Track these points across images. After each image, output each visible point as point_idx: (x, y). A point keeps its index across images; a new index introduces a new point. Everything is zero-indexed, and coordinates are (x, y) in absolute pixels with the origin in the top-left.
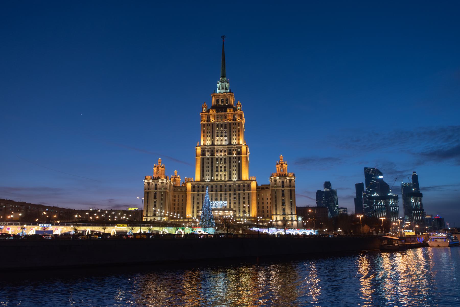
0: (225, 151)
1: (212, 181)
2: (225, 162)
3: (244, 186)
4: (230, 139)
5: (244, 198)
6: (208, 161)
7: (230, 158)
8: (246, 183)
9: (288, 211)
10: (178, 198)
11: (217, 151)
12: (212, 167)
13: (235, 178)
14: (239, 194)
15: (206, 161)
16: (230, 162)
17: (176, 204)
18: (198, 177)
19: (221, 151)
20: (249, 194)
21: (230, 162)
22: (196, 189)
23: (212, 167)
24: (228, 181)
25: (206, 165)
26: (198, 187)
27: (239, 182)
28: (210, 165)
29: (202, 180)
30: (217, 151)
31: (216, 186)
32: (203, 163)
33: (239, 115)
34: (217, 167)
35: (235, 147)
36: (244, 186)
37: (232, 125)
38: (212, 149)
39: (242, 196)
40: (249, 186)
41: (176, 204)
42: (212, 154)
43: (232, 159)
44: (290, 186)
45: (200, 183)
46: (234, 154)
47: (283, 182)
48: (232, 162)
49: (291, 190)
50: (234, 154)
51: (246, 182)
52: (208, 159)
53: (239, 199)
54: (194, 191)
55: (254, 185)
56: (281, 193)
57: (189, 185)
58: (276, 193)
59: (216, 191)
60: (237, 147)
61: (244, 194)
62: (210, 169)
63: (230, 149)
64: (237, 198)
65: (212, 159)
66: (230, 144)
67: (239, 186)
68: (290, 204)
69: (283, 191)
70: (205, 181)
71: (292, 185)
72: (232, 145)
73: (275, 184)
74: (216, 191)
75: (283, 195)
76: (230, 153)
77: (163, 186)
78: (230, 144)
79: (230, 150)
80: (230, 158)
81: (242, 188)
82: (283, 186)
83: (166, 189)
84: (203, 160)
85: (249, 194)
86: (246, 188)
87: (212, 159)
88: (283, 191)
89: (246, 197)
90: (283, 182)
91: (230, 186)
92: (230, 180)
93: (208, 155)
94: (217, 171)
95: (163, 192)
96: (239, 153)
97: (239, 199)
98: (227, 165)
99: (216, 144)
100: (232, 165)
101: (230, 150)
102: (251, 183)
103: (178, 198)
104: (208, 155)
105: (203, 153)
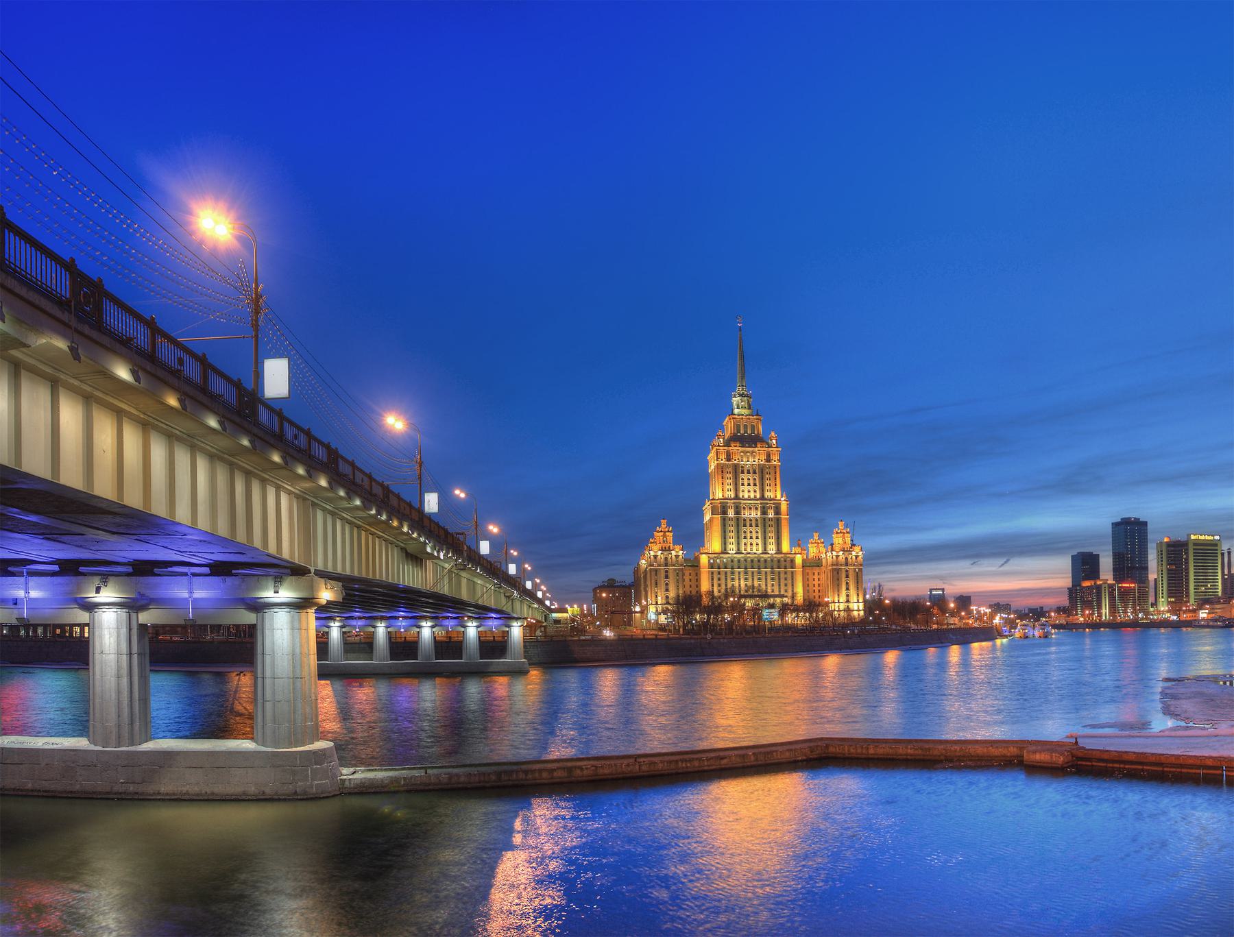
1: (739, 552)
4: (762, 490)
13: (772, 548)
18: (716, 546)
29: (724, 551)
40: (792, 561)
46: (771, 514)
50: (771, 514)
55: (799, 560)
56: (844, 575)
57: (704, 559)
66: (762, 498)
67: (779, 561)
76: (764, 513)
78: (762, 498)
81: (783, 564)
84: (724, 522)
89: (789, 576)
91: (766, 561)
92: (765, 552)
93: (731, 513)
96: (778, 512)
104: (731, 513)
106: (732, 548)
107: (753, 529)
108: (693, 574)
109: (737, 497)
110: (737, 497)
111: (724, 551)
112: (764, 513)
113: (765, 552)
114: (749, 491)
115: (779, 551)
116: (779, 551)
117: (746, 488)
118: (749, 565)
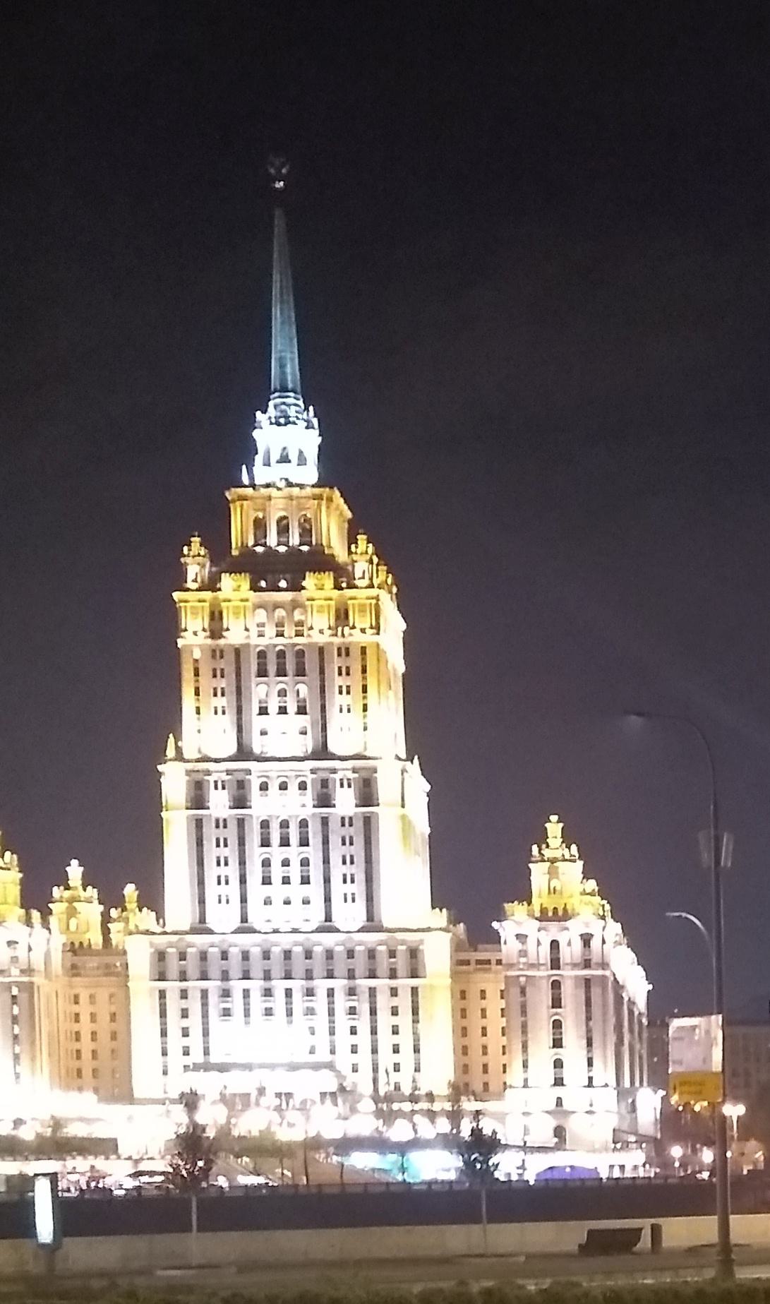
0: (303, 786)
2: (304, 842)
3: (392, 954)
5: (395, 1012)
6: (222, 833)
7: (325, 821)
8: (403, 942)
9: (575, 1070)
10: (94, 1027)
11: (264, 787)
12: (242, 863)
13: (350, 915)
14: (372, 992)
15: (210, 833)
16: (326, 842)
17: (86, 1055)
19: (283, 787)
20: (414, 991)
21: (326, 842)
22: (173, 966)
23: (242, 863)
24: (320, 930)
25: (211, 853)
26: (183, 957)
27: (372, 938)
28: (231, 852)
29: (201, 927)
30: (264, 787)
31: (266, 955)
32: (200, 843)
33: (362, 609)
34: (266, 863)
35: (345, 770)
36: (392, 954)
37: (335, 662)
38: (240, 776)
39: (383, 1002)
40: (414, 953)
41: (86, 1055)
42: (240, 802)
43: (334, 825)
44: (587, 964)
45: (189, 938)
46: (345, 802)
47: (555, 945)
48: (335, 840)
49: (588, 982)
50: (345, 802)
51: (399, 936)
52: (221, 824)
53: (373, 1012)
54: (162, 977)
56: (546, 996)
58: (523, 992)
59: (267, 976)
60: (354, 771)
61: (394, 992)
62: (232, 871)
63: (324, 775)
64: (364, 1008)
65: (241, 822)
66: (322, 752)
68: (585, 1041)
69: (556, 985)
70: (210, 932)
71: (595, 958)
72: (333, 757)
73: (523, 953)
74: (267, 976)
75: (557, 1003)
76: (324, 800)
77: (14, 959)
78: (322, 752)
79: (325, 783)
80: (325, 821)
81: (383, 963)
82: (555, 963)
83: (28, 971)
85: (414, 991)
86: (401, 963)
87: (241, 822)
88: (556, 985)
89: (404, 1002)
90: (555, 945)
91: (329, 955)
92: (328, 926)
93: (219, 803)
94: (267, 881)
95: (18, 984)
96: (367, 796)
97: (373, 1012)
98: (313, 852)
99: (257, 750)
100: (335, 859)
101: (325, 783)
102: (421, 942)
103: (94, 1027)
104: (219, 803)
105: (198, 800)
106: (223, 917)
107: (294, 852)
108: (102, 995)
109: (244, 753)
110: (244, 753)
111: (201, 927)
112: (324, 800)
113: (328, 926)
114: (283, 734)
115: (372, 923)
116: (372, 923)
117: (273, 720)
118: (277, 967)
